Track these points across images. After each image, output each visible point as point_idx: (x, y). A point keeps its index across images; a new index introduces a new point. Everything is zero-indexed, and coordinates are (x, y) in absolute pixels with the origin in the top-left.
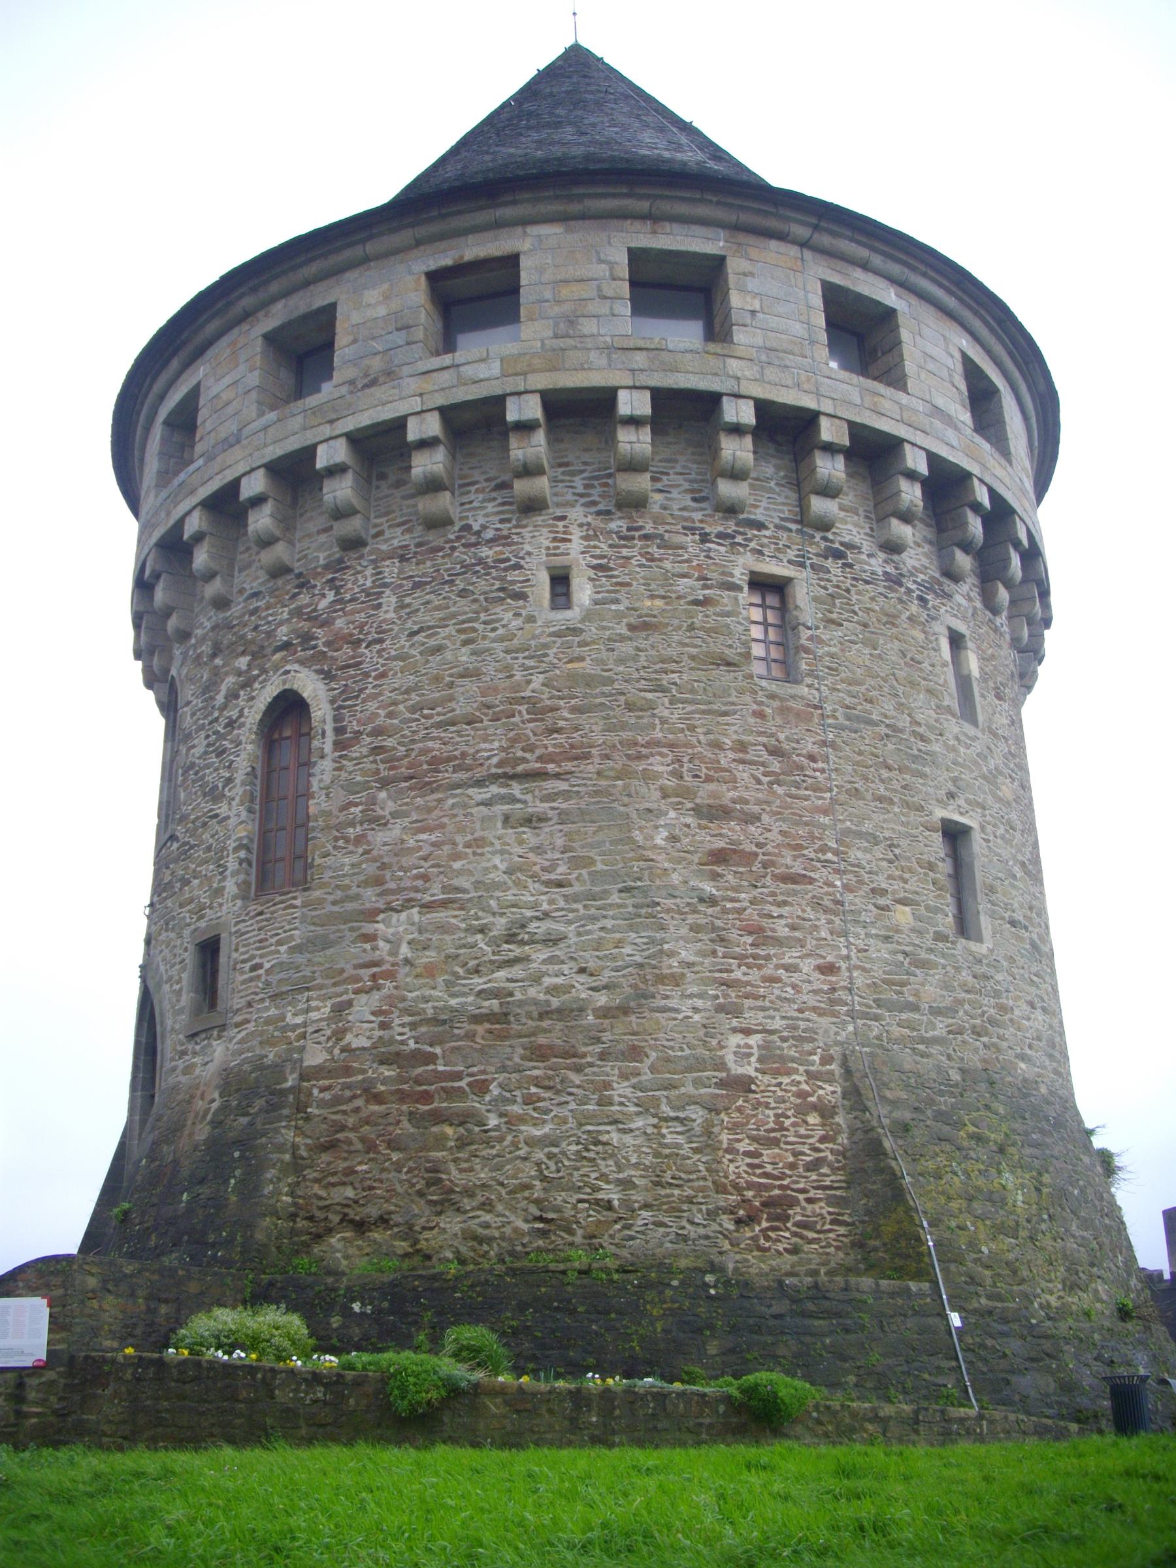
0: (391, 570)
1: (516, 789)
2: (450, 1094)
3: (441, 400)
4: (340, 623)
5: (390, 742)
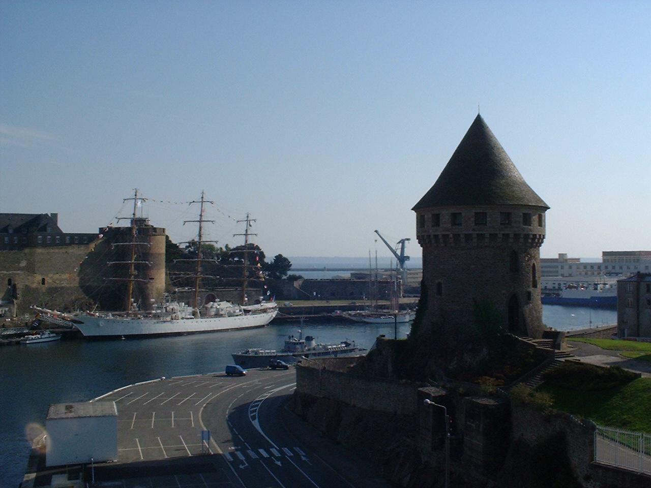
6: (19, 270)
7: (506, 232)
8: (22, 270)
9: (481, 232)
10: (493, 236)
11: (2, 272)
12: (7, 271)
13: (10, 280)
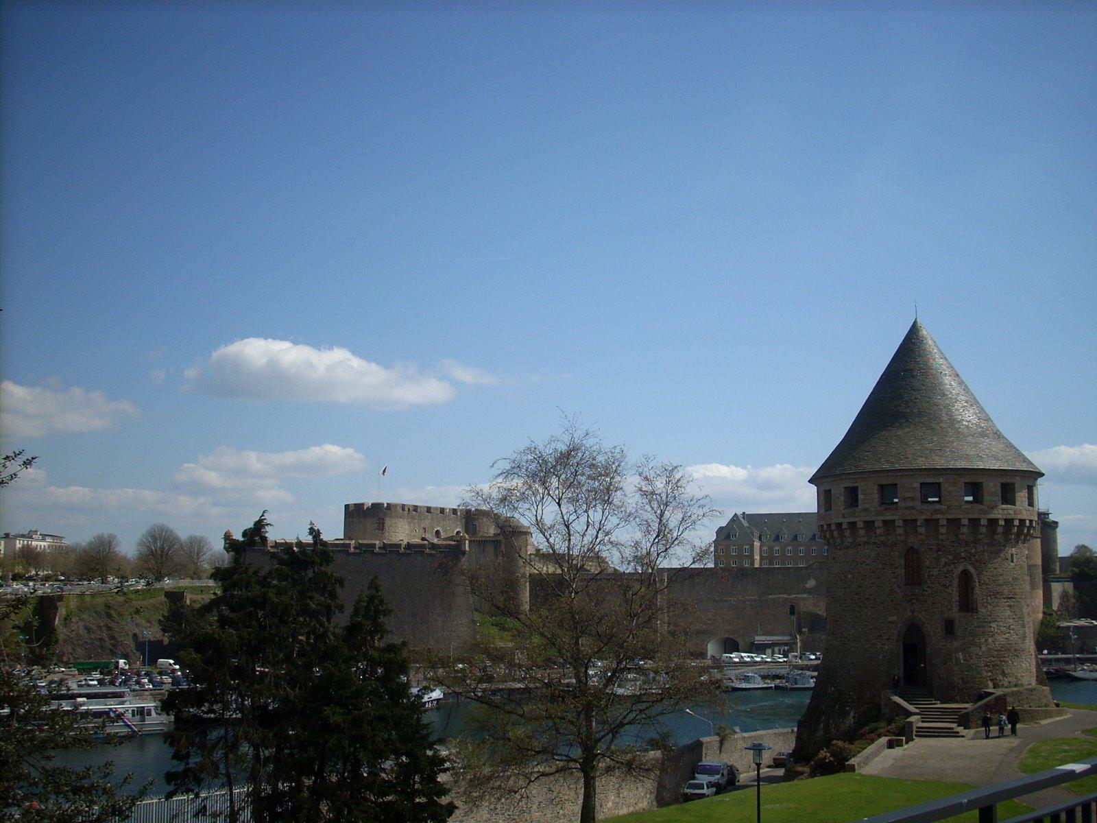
0: (986, 547)
1: (1008, 600)
2: (1005, 657)
3: (1005, 517)
4: (977, 557)
5: (989, 587)
6: (805, 593)
7: (889, 518)
8: (809, 593)
9: (852, 520)
10: (869, 525)
11: (782, 596)
12: (789, 594)
13: (792, 608)
